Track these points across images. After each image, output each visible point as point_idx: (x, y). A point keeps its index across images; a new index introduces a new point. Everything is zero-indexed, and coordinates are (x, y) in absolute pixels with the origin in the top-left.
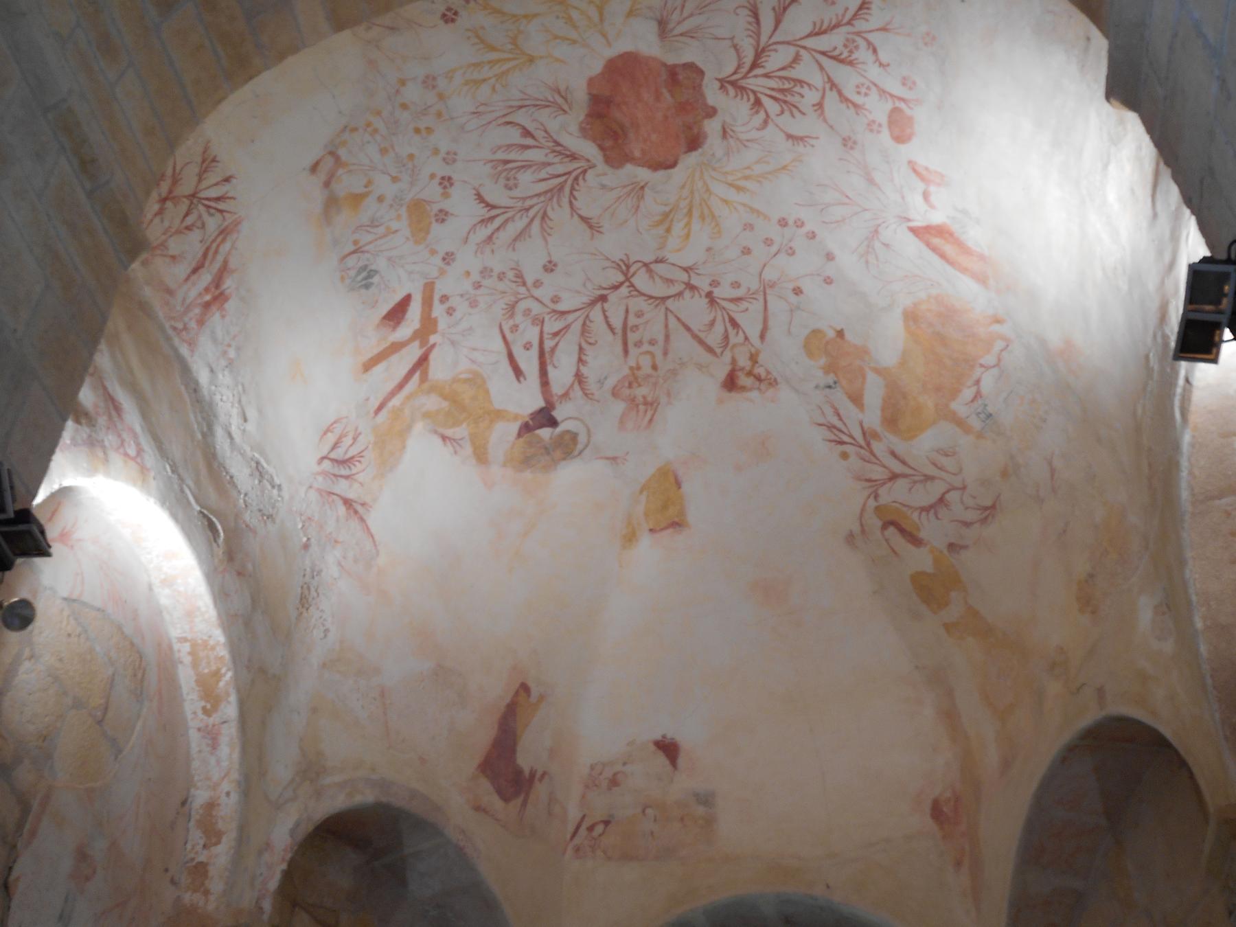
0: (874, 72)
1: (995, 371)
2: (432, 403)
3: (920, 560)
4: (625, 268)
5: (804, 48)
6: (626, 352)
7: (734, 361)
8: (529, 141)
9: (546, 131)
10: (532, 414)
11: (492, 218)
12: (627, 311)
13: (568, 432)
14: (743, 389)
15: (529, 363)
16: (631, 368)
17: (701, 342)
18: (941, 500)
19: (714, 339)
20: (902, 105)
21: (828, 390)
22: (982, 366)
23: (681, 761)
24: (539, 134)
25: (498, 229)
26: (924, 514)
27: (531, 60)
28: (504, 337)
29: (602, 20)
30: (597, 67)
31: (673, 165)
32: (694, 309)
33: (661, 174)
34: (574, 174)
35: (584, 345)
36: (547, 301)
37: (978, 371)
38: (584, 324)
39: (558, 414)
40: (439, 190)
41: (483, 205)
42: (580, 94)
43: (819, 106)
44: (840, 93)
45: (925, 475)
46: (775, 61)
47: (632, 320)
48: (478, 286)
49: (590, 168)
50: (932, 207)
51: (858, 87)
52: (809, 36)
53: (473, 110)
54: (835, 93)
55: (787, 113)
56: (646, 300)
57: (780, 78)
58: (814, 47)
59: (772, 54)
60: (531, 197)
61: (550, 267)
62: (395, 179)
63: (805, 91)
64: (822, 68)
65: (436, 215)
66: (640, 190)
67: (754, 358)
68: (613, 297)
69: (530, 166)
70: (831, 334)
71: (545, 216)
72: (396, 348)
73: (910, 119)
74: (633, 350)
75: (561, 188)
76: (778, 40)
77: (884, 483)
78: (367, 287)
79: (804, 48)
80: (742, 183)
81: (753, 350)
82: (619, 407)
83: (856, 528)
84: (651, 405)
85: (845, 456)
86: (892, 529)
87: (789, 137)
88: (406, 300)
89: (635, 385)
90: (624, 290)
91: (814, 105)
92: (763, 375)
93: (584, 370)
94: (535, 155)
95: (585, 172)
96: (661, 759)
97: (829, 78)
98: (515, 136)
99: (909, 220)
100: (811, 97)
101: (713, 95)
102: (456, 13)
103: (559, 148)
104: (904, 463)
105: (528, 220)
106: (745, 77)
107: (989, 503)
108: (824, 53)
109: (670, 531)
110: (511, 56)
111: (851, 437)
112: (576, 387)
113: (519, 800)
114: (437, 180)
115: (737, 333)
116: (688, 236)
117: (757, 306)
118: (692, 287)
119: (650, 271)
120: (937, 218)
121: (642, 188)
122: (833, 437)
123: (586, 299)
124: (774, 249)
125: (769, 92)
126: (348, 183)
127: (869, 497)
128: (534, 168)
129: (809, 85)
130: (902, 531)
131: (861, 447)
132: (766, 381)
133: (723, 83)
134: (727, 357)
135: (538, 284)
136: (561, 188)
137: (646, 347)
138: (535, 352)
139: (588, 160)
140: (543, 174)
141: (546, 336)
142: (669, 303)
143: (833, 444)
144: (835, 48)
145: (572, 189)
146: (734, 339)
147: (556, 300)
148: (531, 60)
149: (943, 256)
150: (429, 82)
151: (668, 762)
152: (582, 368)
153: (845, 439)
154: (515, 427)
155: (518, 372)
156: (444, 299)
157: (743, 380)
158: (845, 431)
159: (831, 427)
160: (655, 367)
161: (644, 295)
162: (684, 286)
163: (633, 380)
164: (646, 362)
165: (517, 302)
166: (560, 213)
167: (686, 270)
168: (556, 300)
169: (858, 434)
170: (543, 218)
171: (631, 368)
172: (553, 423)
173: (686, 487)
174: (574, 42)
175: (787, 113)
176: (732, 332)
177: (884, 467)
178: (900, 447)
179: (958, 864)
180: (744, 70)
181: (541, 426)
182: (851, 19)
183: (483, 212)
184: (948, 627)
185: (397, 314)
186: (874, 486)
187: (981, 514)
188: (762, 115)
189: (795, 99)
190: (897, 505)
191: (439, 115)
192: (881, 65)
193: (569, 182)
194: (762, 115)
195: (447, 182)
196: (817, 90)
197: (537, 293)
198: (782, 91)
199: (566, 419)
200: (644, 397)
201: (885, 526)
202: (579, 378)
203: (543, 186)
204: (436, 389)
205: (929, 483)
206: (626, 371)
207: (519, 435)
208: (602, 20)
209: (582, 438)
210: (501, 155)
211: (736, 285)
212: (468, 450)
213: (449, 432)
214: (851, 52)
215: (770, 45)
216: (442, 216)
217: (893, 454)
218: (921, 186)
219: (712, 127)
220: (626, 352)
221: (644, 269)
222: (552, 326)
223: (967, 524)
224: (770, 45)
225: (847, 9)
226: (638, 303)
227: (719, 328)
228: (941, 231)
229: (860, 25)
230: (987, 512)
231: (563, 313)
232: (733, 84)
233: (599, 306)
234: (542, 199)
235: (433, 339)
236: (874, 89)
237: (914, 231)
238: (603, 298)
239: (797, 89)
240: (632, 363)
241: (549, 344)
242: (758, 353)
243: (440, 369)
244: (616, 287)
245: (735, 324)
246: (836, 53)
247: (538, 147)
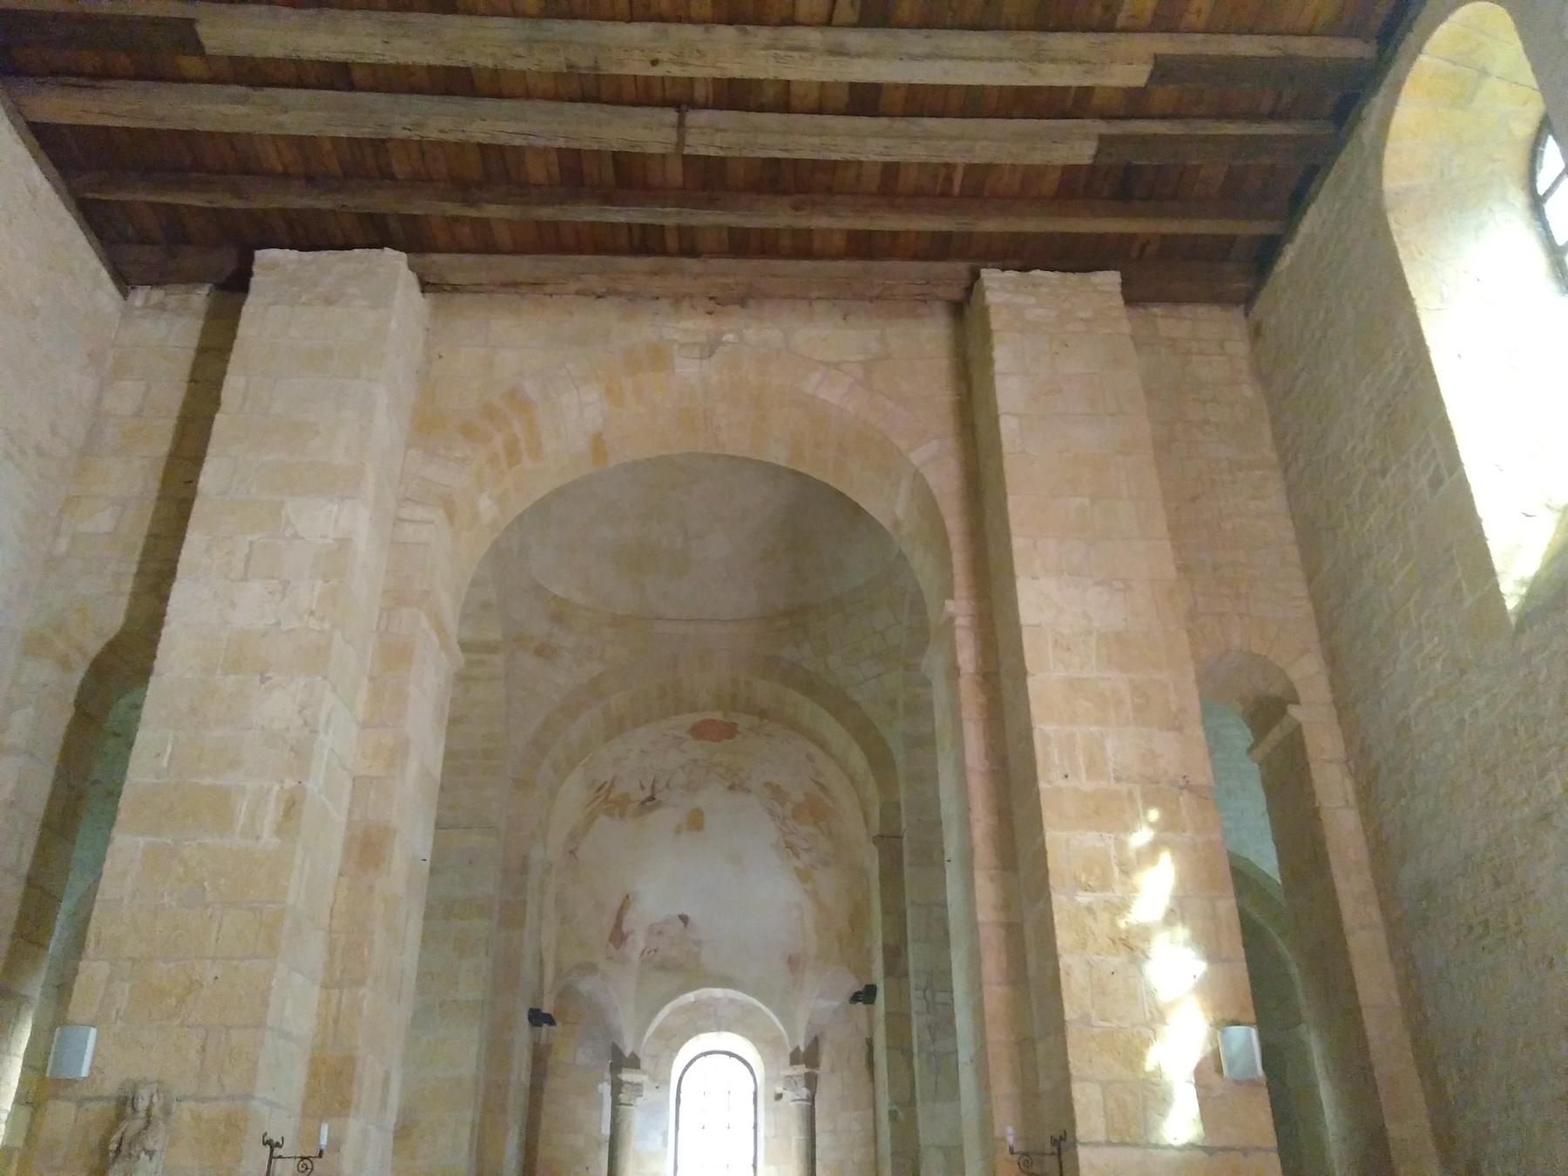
3: (800, 864)
15: (648, 786)
23: (689, 925)
39: (658, 797)
86: (789, 850)
88: (606, 783)
96: (681, 924)
154: (637, 804)
159: (770, 810)
172: (654, 799)
185: (599, 789)
202: (667, 785)
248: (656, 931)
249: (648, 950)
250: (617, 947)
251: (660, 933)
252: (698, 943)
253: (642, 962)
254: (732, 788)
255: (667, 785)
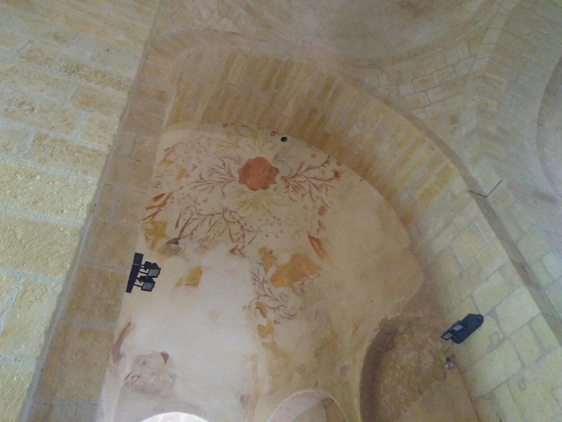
0: (323, 195)
1: (311, 280)
2: (150, 227)
3: (263, 322)
4: (225, 210)
5: (309, 180)
6: (209, 231)
7: (237, 246)
8: (223, 167)
9: (229, 166)
10: (173, 239)
11: (199, 182)
12: (217, 221)
13: (179, 247)
14: (235, 254)
16: (207, 236)
17: (231, 236)
18: (278, 307)
19: (235, 237)
20: (326, 206)
21: (259, 264)
22: (308, 277)
23: (168, 361)
24: (227, 166)
25: (199, 185)
26: (271, 309)
27: (238, 147)
28: (181, 213)
29: (263, 146)
30: (254, 157)
31: (256, 190)
32: (235, 228)
33: (251, 191)
34: (229, 180)
35: (199, 225)
36: (198, 210)
37: (306, 278)
38: (204, 219)
40: (192, 168)
41: (200, 177)
42: (244, 162)
43: (304, 195)
44: (311, 195)
45: (276, 299)
46: (299, 179)
47: (217, 224)
48: (184, 198)
49: (234, 181)
50: (318, 233)
51: (317, 196)
52: (312, 178)
53: (215, 152)
54: (310, 194)
55: (294, 193)
56: (224, 220)
57: (298, 183)
58: (311, 181)
59: (300, 177)
60: (213, 181)
61: (205, 201)
62: (183, 161)
63: (302, 190)
64: (310, 187)
65: (186, 175)
66: (243, 192)
67: (243, 247)
68: (216, 215)
69: (218, 173)
70: (269, 250)
71: (213, 187)
72: (152, 207)
73: (326, 211)
74: (211, 232)
75: (223, 182)
76: (304, 175)
77: (263, 296)
78: (156, 187)
79: (309, 180)
80: (270, 203)
81: (244, 245)
82: (197, 245)
83: (248, 305)
84: (206, 248)
85: (254, 284)
86: (258, 310)
87: (291, 198)
89: (205, 241)
90: (221, 215)
91: (302, 194)
92: (243, 252)
93: (195, 232)
94: (222, 171)
95: (232, 181)
96: (162, 359)
97: (311, 190)
98: (220, 163)
99: (310, 234)
100: (303, 192)
101: (278, 178)
102: (227, 126)
103: (229, 172)
104: (271, 293)
105: (208, 186)
106: (289, 179)
107: (292, 314)
108: (313, 184)
109: (192, 286)
110: (233, 143)
111: (259, 279)
112: (189, 236)
113: (116, 364)
114: (193, 166)
115: (243, 239)
116: (247, 209)
117: (253, 234)
118: (238, 222)
119: (231, 213)
120: (317, 236)
121: (244, 192)
122: (254, 278)
123: (209, 214)
124: (267, 223)
125: (293, 186)
126: (172, 157)
127: (256, 298)
128: (219, 174)
129: (304, 189)
130: (261, 311)
131: (260, 284)
132: (243, 255)
133: (283, 178)
134: (236, 244)
135: (199, 204)
136: (223, 182)
137: (215, 232)
138: (185, 221)
139: (234, 179)
140: (221, 177)
141: (191, 219)
142: (230, 224)
143: (253, 279)
144: (317, 185)
145: (226, 184)
146: (241, 239)
147: (200, 210)
148: (238, 147)
149: (313, 246)
150: (209, 140)
151: (164, 361)
152: (194, 231)
153: (257, 279)
154: (166, 241)
155: (177, 226)
156: (173, 198)
157: (237, 252)
158: (258, 277)
159: (254, 275)
160: (214, 238)
161: (224, 218)
162: (237, 221)
163: (205, 240)
164: (212, 236)
165: (190, 206)
166: (218, 188)
167: (241, 217)
168: (200, 210)
169: (261, 280)
170: (213, 187)
171: (207, 236)
172: (177, 243)
173: (203, 275)
174: (252, 148)
175: (294, 193)
176: (241, 238)
177: (265, 292)
178: (272, 289)
179: (245, 417)
180: (290, 177)
181: (174, 243)
182: (325, 180)
183: (198, 179)
184: (263, 344)
186: (259, 295)
187: (289, 316)
188: (287, 190)
189: (298, 191)
190: (263, 304)
191: (206, 149)
192: (327, 195)
193: (226, 182)
194: (287, 190)
195: (195, 167)
196: (305, 191)
197: (197, 206)
198: (296, 187)
199: (182, 244)
200: (206, 245)
201: (256, 308)
202: (192, 233)
203: (219, 180)
204: (153, 223)
205: (276, 301)
206: (205, 236)
207: (166, 244)
208: (263, 146)
209: (182, 251)
210: (213, 167)
211: (251, 227)
212: (150, 243)
213: (148, 236)
214: (321, 187)
215: (300, 175)
216: (188, 176)
217: (269, 289)
218: (318, 227)
219: (272, 186)
220: (209, 231)
221: (229, 212)
222: (195, 216)
223: (282, 317)
224: (300, 175)
225: (326, 177)
226: (223, 221)
227: (238, 236)
228: (317, 240)
229: (327, 183)
230: (291, 316)
231: (200, 214)
232: (284, 178)
233: (210, 217)
234: (216, 183)
235: (162, 208)
236: (321, 199)
237: (309, 237)
238: (213, 215)
239: (301, 188)
240: (208, 234)
241: (190, 221)
242: (245, 246)
243: (158, 218)
244: (218, 214)
245: (244, 236)
246: (316, 186)
247: (224, 169)
248: (142, 361)
249: (131, 375)
250: (114, 362)
251: (144, 363)
252: (173, 376)
253: (126, 384)
254: (232, 251)
255: (192, 233)
